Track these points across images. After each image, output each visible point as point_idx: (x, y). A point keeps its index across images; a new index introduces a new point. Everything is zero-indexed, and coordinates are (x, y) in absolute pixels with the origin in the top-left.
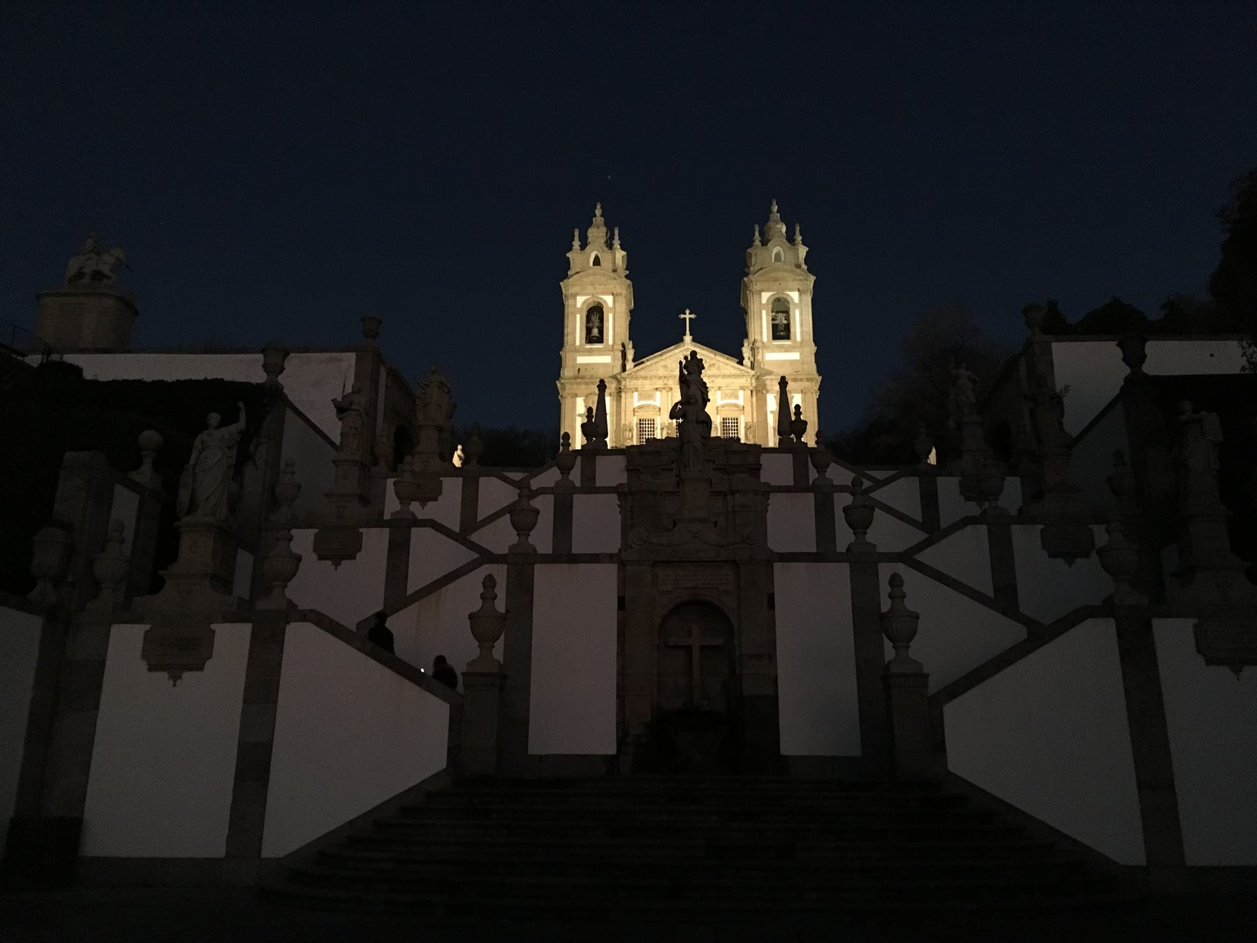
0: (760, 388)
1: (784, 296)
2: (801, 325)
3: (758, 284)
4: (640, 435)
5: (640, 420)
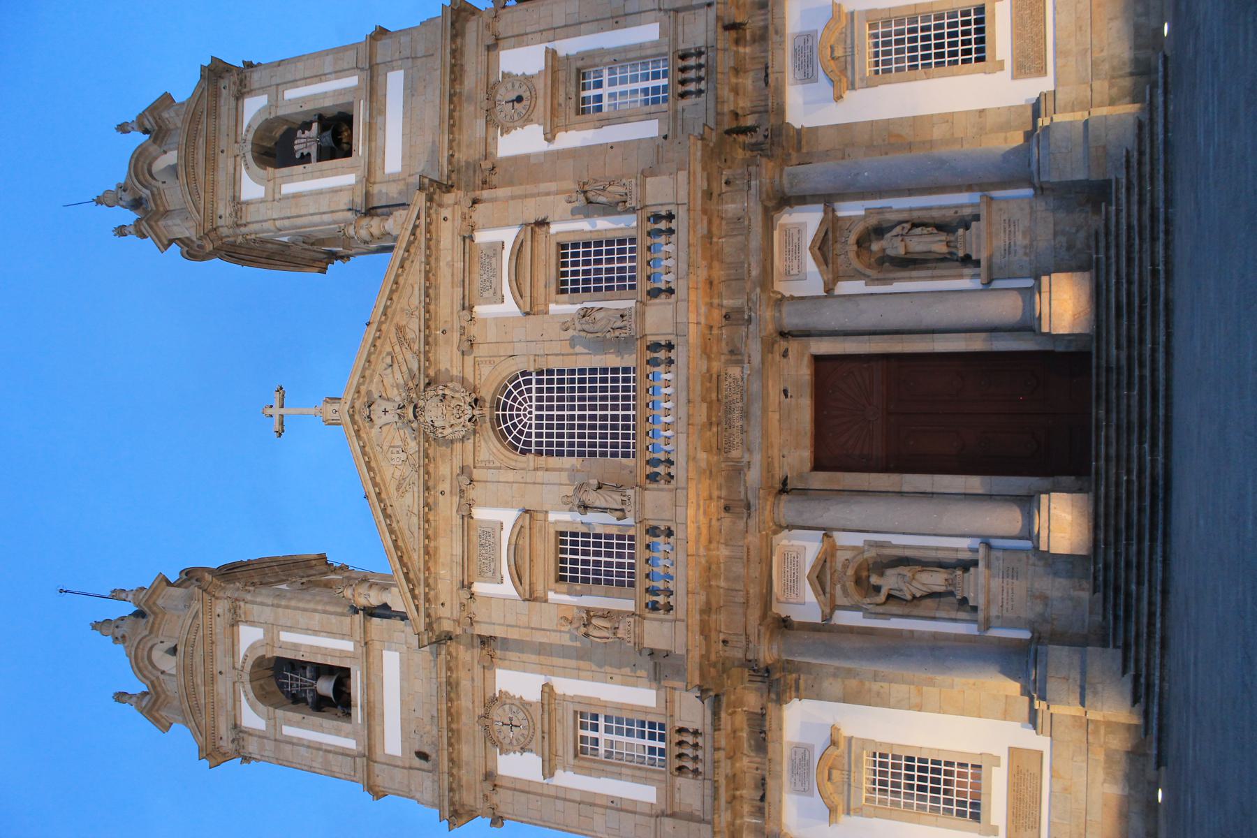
0: (478, 182)
1: (250, 137)
2: (320, 77)
3: (221, 211)
4: (609, 582)
5: (563, 578)
